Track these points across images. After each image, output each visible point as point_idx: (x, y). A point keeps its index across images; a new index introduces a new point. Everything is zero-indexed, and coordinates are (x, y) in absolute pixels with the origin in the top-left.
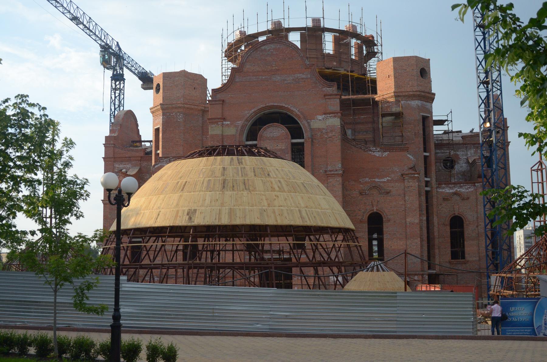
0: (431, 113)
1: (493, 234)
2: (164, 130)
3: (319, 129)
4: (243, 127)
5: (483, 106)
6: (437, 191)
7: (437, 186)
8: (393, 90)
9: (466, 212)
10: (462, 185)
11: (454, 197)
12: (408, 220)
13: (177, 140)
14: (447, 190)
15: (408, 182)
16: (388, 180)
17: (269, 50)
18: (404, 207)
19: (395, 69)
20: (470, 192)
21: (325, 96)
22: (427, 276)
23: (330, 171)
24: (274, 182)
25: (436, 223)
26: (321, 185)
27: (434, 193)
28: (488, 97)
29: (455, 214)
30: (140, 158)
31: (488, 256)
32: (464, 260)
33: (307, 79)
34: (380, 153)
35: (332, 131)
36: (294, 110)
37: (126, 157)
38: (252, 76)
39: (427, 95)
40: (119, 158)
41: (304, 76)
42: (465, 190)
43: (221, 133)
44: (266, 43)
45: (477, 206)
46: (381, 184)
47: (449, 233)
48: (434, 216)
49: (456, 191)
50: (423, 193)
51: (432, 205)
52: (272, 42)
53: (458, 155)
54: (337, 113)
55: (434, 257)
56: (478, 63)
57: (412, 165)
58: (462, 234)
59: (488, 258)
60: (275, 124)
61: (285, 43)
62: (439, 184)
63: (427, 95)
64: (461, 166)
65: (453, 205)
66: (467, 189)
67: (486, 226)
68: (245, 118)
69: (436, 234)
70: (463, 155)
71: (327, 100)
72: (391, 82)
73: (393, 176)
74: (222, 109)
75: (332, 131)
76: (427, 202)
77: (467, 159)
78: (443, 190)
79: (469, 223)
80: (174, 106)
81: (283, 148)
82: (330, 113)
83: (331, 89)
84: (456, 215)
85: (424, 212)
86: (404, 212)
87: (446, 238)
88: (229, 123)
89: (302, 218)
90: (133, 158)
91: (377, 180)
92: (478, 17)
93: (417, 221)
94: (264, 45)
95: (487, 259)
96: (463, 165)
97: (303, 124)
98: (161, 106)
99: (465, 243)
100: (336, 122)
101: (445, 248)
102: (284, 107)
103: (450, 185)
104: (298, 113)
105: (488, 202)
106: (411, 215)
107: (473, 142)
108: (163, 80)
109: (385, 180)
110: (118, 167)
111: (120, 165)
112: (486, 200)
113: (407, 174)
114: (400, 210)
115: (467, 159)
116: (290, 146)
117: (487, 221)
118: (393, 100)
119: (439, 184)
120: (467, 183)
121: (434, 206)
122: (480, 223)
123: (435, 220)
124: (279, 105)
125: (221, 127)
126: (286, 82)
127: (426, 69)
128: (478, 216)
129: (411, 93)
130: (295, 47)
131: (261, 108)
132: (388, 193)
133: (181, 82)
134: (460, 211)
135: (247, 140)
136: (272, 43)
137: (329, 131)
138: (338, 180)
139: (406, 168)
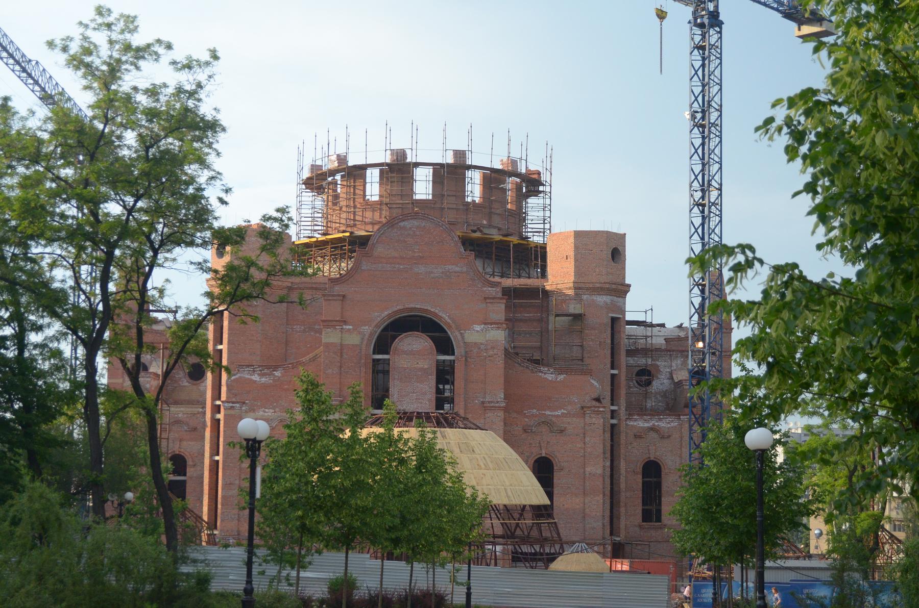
0: (623, 312)
3: (475, 343)
4: (371, 335)
5: (696, 316)
6: (626, 424)
8: (572, 279)
12: (588, 469)
15: (590, 417)
17: (410, 228)
19: (576, 248)
21: (485, 298)
23: (489, 402)
24: (479, 459)
25: (623, 471)
26: (518, 457)
27: (623, 427)
28: (702, 305)
34: (554, 376)
35: (493, 348)
36: (444, 316)
39: (620, 287)
41: (458, 269)
42: (666, 423)
43: (340, 341)
46: (554, 419)
47: (641, 485)
50: (608, 429)
51: (619, 445)
53: (658, 366)
54: (502, 324)
55: (619, 518)
56: (693, 151)
57: (595, 395)
58: (659, 485)
62: (630, 416)
63: (620, 287)
64: (660, 384)
66: (669, 423)
68: (375, 323)
69: (623, 486)
70: (665, 366)
72: (570, 267)
73: (569, 408)
74: (342, 308)
75: (493, 348)
76: (612, 440)
77: (671, 374)
78: (635, 424)
81: (426, 367)
82: (491, 324)
85: (608, 455)
88: (351, 327)
89: (508, 497)
91: (548, 413)
92: (696, 191)
93: (600, 471)
96: (665, 381)
97: (454, 335)
99: (663, 499)
100: (499, 335)
104: (449, 321)
107: (680, 349)
109: (559, 413)
113: (589, 407)
115: (671, 374)
116: (434, 365)
118: (571, 292)
119: (630, 415)
123: (623, 466)
126: (432, 275)
127: (620, 248)
129: (598, 285)
132: (562, 431)
134: (658, 454)
135: (374, 353)
137: (489, 347)
139: (587, 398)
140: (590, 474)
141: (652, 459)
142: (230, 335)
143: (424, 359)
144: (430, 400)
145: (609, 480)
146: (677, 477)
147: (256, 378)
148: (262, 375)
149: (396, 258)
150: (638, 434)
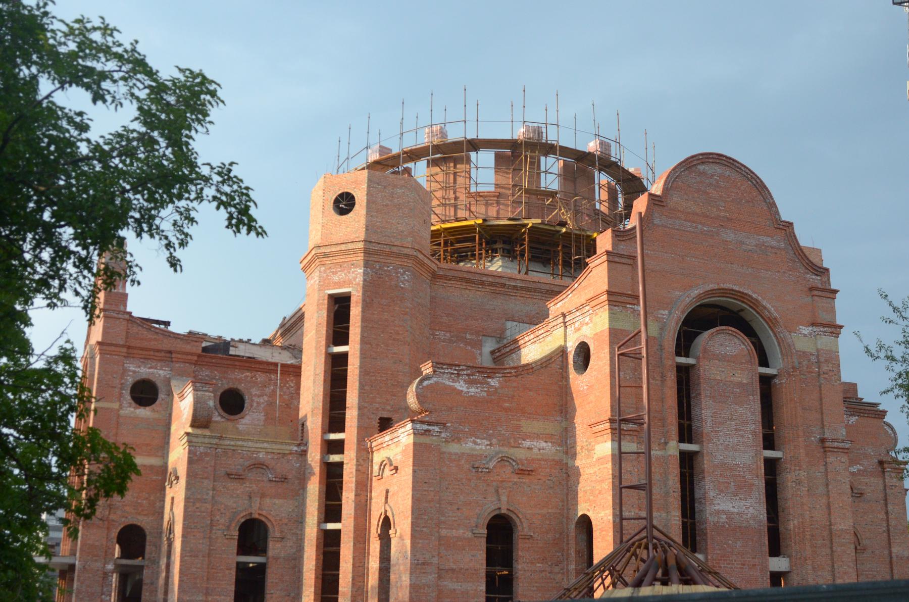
2: (368, 300)
3: (804, 353)
13: (397, 328)
16: (859, 470)
17: (712, 175)
21: (811, 289)
30: (195, 358)
33: (779, 249)
36: (769, 306)
37: (158, 351)
38: (685, 220)
40: (142, 349)
41: (774, 243)
44: (707, 160)
52: (718, 161)
60: (730, 328)
61: (740, 169)
71: (816, 298)
73: (866, 463)
80: (395, 249)
82: (824, 325)
83: (819, 278)
90: (179, 356)
94: (703, 163)
98: (365, 245)
102: (750, 296)
106: (898, 541)
108: (369, 187)
110: (134, 372)
111: (139, 367)
124: (742, 290)
125: (632, 315)
126: (744, 247)
130: (757, 183)
131: (711, 290)
133: (409, 202)
136: (716, 163)
138: (843, 460)
140: (897, 556)
142: (364, 329)
143: (742, 369)
144: (754, 433)
147: (461, 386)
148: (470, 383)
149: (697, 214)
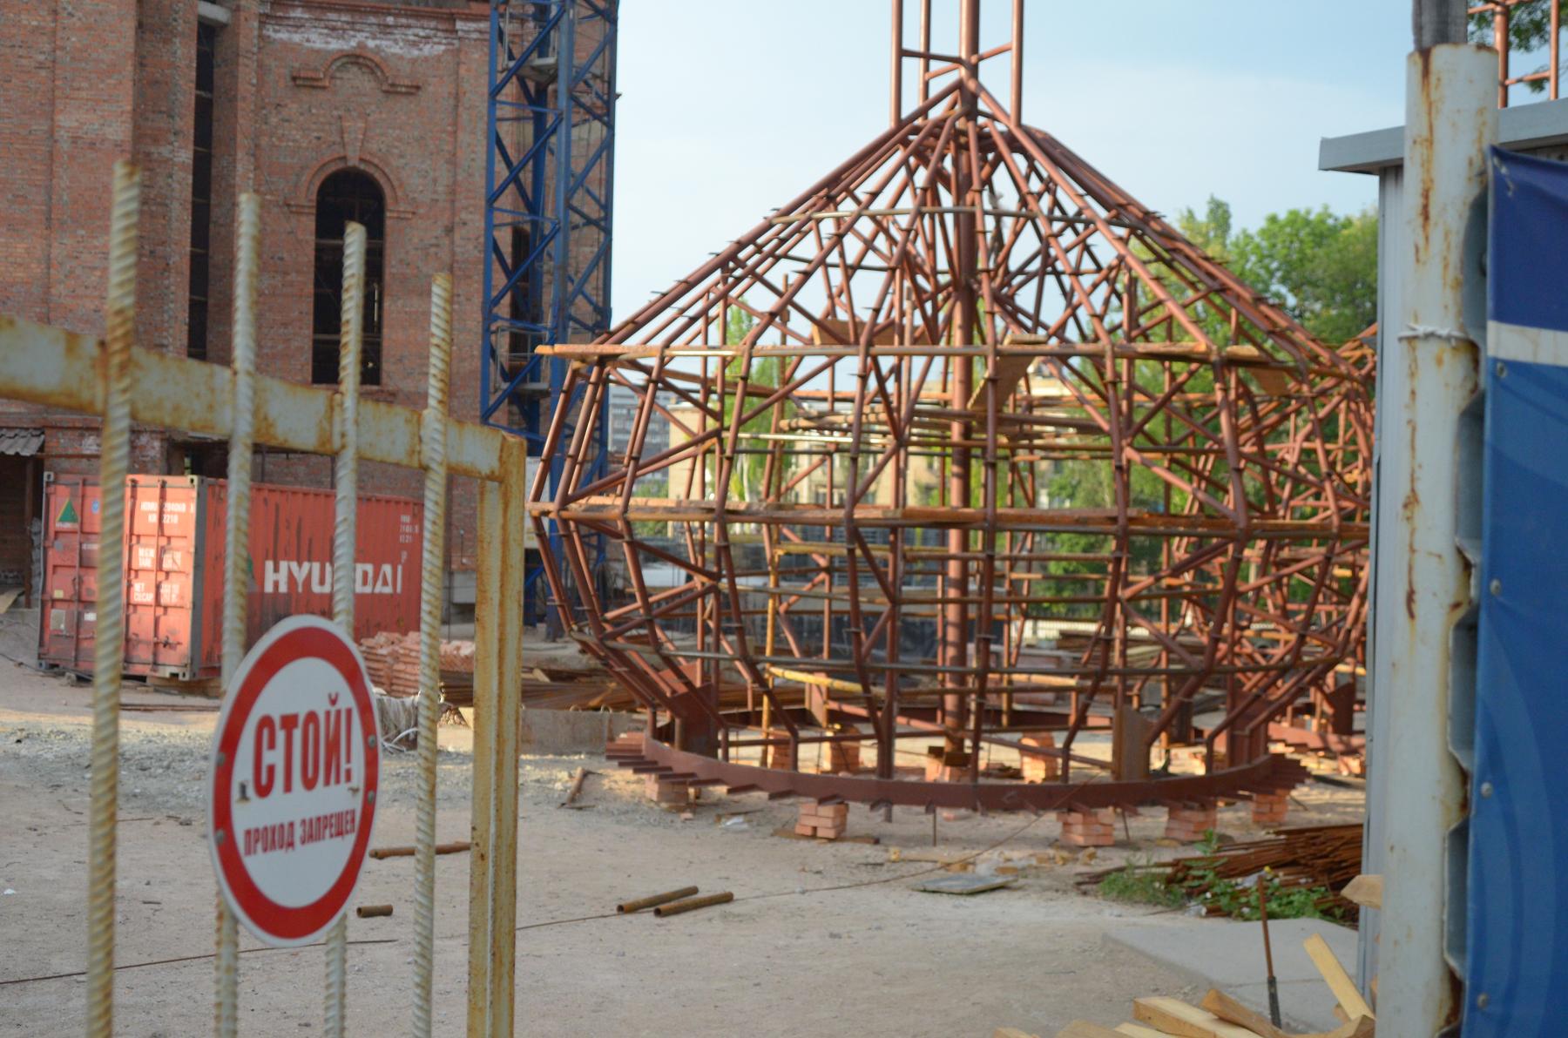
1: (520, 239)
7: (267, 9)
9: (401, 156)
10: (390, 20)
11: (346, 76)
12: (67, 120)
14: (313, 37)
18: (47, 47)
20: (426, 59)
22: (157, 444)
29: (344, 158)
31: (492, 353)
32: (375, 388)
45: (455, 132)
48: (240, 155)
49: (361, 45)
51: (233, 100)
59: (492, 368)
65: (340, 117)
66: (414, 44)
67: (492, 198)
78: (297, 38)
79: (409, 209)
84: (351, 163)
86: (43, 73)
87: (293, 277)
95: (485, 366)
101: (285, 325)
103: (332, 16)
105: (512, 73)
106: (84, 94)
112: (503, 61)
114: (24, 62)
117: (502, 171)
120: (417, 15)
121: (241, 104)
122: (464, 215)
128: (455, 183)
140: (75, 140)
141: (353, 162)
145: (187, 217)
146: (439, 232)
150: (303, 74)
